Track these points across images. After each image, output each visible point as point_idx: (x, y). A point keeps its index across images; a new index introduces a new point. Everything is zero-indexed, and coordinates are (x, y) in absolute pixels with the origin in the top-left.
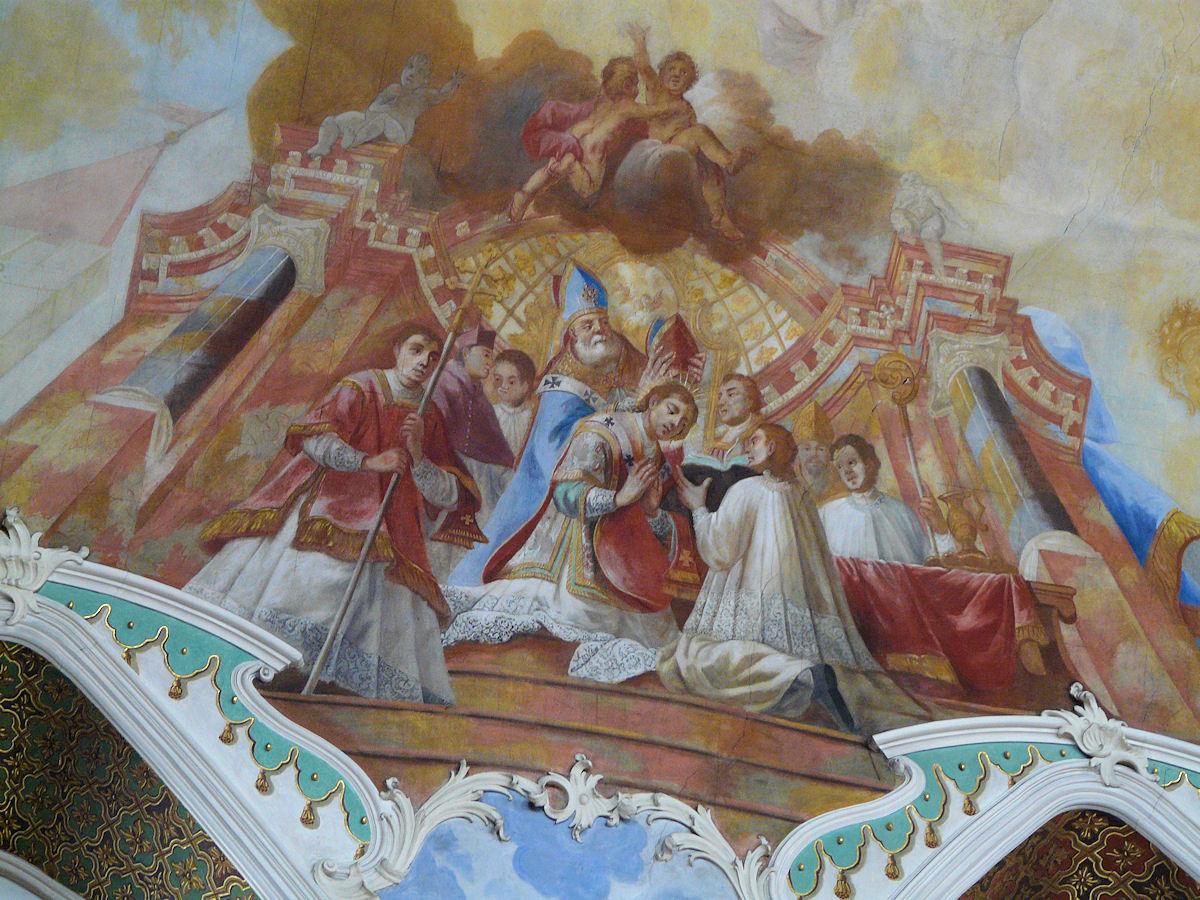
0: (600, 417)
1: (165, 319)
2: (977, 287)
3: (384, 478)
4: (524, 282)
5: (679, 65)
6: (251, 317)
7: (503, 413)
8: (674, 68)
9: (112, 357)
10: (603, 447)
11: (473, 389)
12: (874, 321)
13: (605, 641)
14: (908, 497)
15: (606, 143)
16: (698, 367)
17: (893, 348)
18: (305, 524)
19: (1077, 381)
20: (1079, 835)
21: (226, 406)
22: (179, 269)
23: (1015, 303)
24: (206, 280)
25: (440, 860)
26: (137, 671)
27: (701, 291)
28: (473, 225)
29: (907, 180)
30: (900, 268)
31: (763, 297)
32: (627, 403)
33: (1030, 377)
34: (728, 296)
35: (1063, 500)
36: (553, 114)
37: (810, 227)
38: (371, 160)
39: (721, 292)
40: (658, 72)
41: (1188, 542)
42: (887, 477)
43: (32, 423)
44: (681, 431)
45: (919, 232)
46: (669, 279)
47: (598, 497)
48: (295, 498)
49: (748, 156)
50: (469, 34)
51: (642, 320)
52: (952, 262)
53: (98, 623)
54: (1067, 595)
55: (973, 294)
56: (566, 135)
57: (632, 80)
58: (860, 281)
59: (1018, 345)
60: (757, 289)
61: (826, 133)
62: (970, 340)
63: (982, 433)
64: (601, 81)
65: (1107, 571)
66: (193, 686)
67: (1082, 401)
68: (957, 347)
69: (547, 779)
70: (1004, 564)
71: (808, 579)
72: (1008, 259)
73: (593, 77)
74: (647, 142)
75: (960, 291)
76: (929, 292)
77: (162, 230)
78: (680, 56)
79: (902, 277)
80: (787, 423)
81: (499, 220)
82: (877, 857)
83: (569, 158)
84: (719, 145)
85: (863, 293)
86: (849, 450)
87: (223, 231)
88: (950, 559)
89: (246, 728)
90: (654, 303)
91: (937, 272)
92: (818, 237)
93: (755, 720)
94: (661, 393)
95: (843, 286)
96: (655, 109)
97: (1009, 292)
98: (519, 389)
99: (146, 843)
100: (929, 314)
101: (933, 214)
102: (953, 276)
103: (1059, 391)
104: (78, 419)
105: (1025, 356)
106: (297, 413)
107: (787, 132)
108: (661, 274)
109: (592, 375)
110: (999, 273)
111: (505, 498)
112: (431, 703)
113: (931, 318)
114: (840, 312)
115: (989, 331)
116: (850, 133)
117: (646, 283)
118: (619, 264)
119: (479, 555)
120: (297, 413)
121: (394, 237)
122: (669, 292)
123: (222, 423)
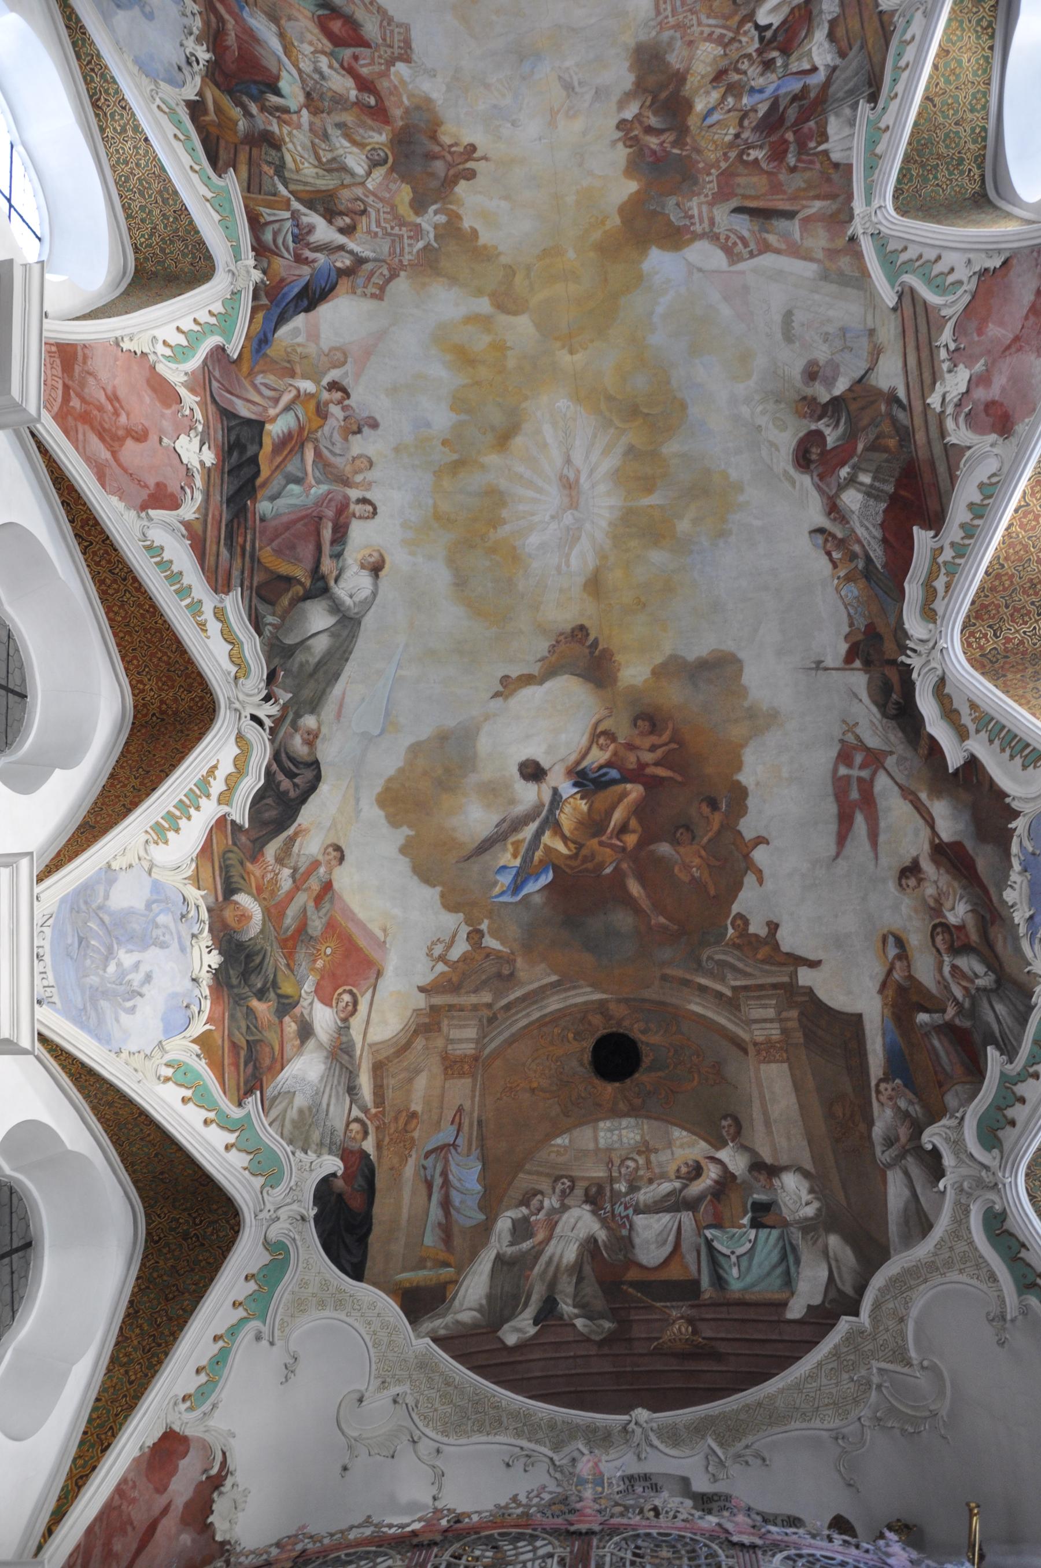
0: (753, 83)
3: (795, 133)
6: (754, 213)
7: (760, 114)
9: (783, 247)
11: (755, 129)
18: (819, 144)
21: (789, 199)
22: (746, 244)
24: (746, 234)
32: (745, 79)
49: (645, 91)
57: (631, 138)
78: (618, 127)
81: (694, 156)
83: (665, 145)
87: (728, 238)
90: (707, 93)
94: (738, 71)
98: (752, 115)
104: (809, 243)
106: (783, 176)
109: (738, 97)
111: (789, 89)
116: (627, 64)
120: (783, 176)
121: (711, 185)
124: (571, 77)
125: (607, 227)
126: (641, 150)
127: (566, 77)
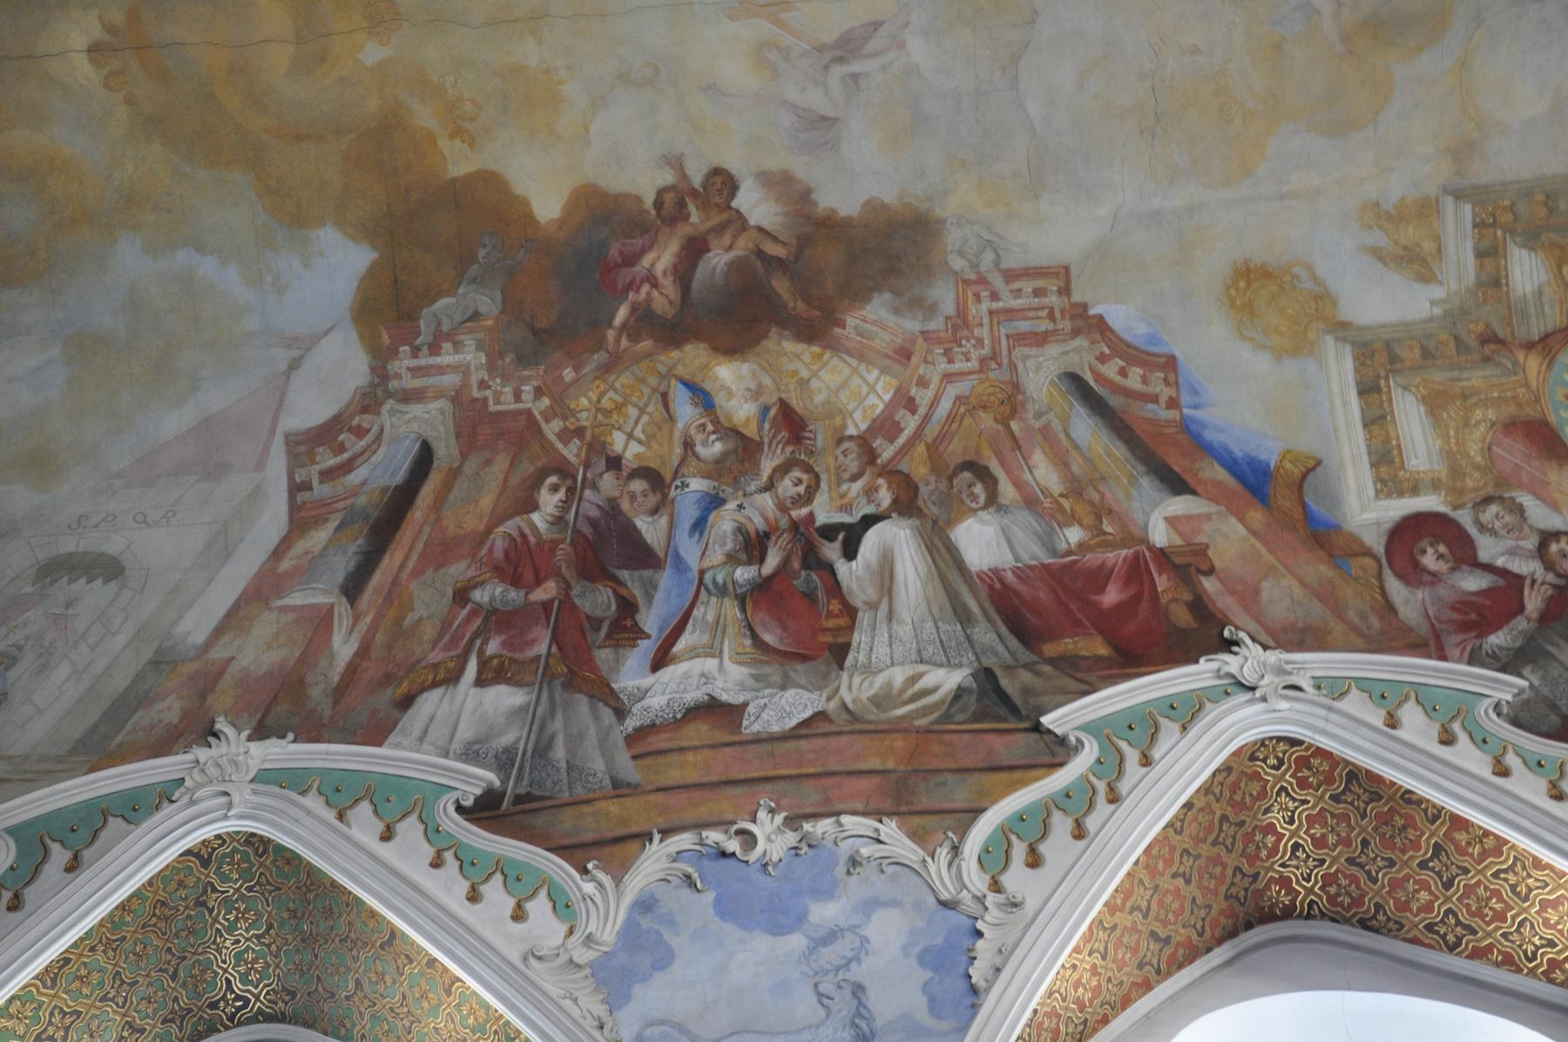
0: (731, 505)
1: (326, 520)
2: (1045, 301)
3: (546, 606)
4: (636, 406)
5: (719, 179)
6: (401, 500)
7: (642, 523)
8: (715, 183)
9: (285, 565)
10: (740, 530)
11: (612, 509)
12: (960, 357)
13: (772, 696)
14: (1030, 502)
15: (675, 266)
16: (810, 439)
17: (983, 376)
18: (483, 664)
19: (1163, 360)
20: (1266, 763)
21: (395, 581)
22: (328, 475)
23: (1085, 306)
24: (355, 477)
25: (645, 923)
26: (350, 827)
27: (795, 373)
28: (577, 369)
29: (952, 224)
30: (970, 303)
31: (853, 362)
32: (753, 486)
33: (1117, 368)
34: (820, 369)
35: (1176, 468)
36: (621, 253)
37: (877, 288)
38: (472, 336)
39: (814, 368)
40: (702, 190)
41: (1304, 476)
42: (1007, 491)
43: (226, 638)
44: (808, 498)
45: (978, 265)
46: (764, 369)
47: (744, 574)
48: (471, 643)
49: (804, 242)
50: (526, 204)
51: (749, 411)
52: (1016, 285)
53: (311, 794)
54: (1201, 551)
55: (1043, 308)
56: (637, 269)
57: (681, 205)
58: (936, 324)
59: (1099, 342)
60: (846, 357)
61: (868, 203)
62: (1053, 350)
63: (1085, 428)
64: (653, 212)
65: (1233, 520)
66: (401, 827)
67: (1172, 377)
68: (1042, 359)
69: (735, 827)
70: (1135, 538)
71: (953, 597)
72: (1067, 269)
73: (647, 212)
74: (710, 255)
75: (1030, 309)
76: (1002, 317)
77: (304, 445)
78: (717, 172)
79: (974, 311)
80: (904, 467)
81: (598, 358)
82: (1061, 824)
84: (775, 239)
85: (942, 335)
86: (967, 476)
87: (360, 432)
88: (1083, 547)
89: (452, 851)
90: (756, 394)
91: (1004, 298)
92: (887, 296)
93: (927, 731)
94: (782, 470)
95: (922, 333)
96: (708, 224)
97: (1077, 297)
98: (653, 500)
99: (387, 978)
100: (1008, 337)
101: (985, 248)
102: (1020, 297)
103: (1147, 373)
104: (266, 625)
105: (1107, 351)
106: (459, 570)
107: (833, 211)
108: (755, 367)
110: (1062, 283)
111: (659, 596)
112: (620, 788)
113: (1011, 341)
114: (926, 357)
115: (1068, 337)
116: (889, 196)
117: (744, 379)
118: (717, 368)
119: (645, 649)
120: (459, 570)
121: (510, 397)
122: (767, 381)
123: (394, 595)
124: (876, 54)
125: (443, 143)
126: (644, 229)
127: (876, 43)
